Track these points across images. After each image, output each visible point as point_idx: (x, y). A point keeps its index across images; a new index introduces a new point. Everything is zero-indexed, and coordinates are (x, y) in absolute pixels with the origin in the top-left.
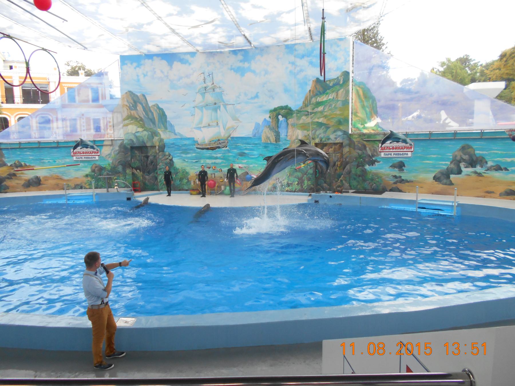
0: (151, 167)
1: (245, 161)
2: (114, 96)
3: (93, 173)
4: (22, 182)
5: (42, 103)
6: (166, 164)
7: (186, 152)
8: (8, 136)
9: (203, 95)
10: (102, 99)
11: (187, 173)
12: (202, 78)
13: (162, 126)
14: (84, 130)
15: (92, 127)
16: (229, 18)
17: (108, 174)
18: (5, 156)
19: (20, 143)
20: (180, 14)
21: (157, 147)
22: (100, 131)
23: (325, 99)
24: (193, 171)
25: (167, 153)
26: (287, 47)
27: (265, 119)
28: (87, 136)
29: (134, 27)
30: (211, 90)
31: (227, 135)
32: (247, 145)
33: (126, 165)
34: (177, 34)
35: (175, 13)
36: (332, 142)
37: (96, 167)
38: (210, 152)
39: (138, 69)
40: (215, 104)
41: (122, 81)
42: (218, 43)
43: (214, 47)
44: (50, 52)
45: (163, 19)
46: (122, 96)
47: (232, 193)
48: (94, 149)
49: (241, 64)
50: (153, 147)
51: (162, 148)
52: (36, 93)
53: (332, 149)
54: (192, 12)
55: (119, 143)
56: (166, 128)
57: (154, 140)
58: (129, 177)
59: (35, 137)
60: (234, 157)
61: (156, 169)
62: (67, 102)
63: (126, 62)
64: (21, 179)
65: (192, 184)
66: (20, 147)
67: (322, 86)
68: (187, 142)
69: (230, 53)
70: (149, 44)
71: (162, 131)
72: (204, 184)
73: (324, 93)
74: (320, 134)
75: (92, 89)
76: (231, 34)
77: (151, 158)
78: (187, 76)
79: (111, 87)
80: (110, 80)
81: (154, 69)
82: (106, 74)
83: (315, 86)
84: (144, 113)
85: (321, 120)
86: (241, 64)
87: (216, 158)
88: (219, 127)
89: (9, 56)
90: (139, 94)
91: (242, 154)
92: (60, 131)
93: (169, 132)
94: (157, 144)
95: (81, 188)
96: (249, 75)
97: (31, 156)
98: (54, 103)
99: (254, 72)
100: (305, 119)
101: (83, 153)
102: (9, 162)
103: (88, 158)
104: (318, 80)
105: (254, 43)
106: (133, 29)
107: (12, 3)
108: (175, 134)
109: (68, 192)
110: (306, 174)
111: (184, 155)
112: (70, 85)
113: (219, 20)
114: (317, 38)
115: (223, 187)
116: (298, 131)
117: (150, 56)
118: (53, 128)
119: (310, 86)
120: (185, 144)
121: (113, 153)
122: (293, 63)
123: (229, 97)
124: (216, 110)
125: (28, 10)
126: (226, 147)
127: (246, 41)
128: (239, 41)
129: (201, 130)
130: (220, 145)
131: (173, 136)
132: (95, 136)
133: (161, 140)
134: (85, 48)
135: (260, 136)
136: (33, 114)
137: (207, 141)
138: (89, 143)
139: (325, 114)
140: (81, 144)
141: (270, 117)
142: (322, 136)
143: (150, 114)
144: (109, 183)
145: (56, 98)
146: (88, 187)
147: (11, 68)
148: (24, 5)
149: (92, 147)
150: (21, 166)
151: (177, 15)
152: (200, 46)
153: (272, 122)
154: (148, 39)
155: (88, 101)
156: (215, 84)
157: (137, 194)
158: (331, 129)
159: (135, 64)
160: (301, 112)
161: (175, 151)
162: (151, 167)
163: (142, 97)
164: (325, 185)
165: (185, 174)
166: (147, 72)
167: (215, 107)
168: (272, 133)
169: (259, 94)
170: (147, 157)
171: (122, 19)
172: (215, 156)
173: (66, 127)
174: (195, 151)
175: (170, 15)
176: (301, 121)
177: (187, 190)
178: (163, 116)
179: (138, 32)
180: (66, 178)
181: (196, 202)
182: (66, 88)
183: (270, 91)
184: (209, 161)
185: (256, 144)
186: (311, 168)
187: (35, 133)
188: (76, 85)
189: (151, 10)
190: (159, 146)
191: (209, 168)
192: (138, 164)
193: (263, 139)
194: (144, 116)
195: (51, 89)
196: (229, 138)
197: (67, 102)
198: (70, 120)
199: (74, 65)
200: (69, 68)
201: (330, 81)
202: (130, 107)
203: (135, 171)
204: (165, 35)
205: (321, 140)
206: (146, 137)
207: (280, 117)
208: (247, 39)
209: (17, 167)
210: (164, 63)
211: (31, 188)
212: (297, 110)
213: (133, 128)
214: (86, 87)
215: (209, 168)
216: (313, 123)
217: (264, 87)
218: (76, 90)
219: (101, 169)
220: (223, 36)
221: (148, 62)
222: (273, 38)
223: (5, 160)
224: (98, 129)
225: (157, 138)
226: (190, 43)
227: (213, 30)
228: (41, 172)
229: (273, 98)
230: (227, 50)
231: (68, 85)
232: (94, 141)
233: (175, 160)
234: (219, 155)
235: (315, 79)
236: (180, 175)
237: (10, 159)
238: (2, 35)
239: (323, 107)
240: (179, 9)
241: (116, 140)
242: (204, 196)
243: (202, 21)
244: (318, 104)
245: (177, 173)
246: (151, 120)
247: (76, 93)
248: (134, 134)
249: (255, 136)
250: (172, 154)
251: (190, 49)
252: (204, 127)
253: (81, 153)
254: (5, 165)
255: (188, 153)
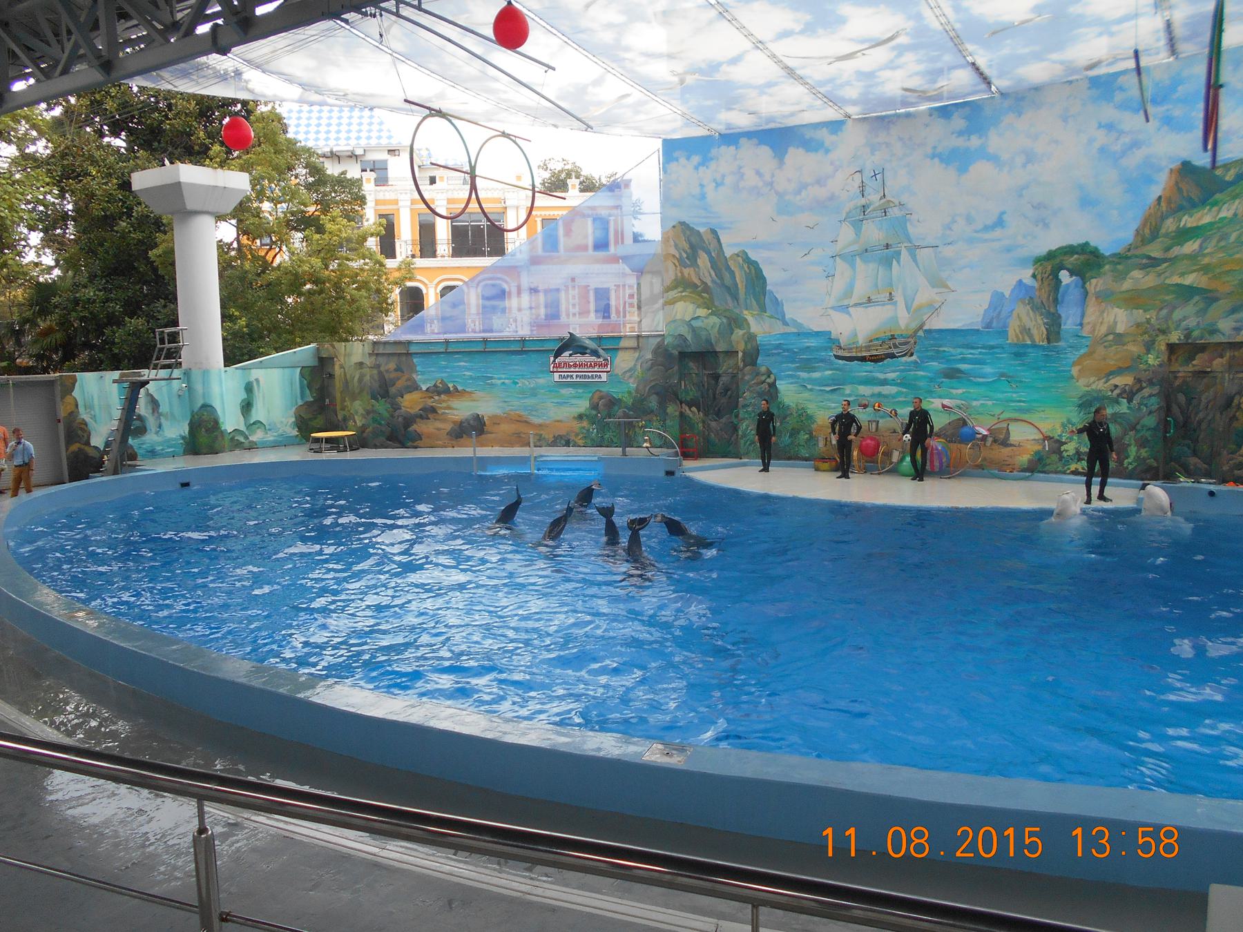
0: (724, 400)
1: (960, 391)
2: (641, 235)
3: (594, 412)
4: (448, 427)
5: (490, 255)
6: (760, 395)
7: (808, 365)
8: (420, 328)
9: (857, 225)
10: (616, 242)
11: (810, 417)
12: (858, 182)
13: (754, 303)
14: (574, 315)
15: (592, 307)
16: (935, 25)
17: (626, 416)
18: (418, 368)
19: (447, 342)
20: (809, 30)
21: (740, 354)
22: (609, 317)
23: (1207, 219)
24: (824, 412)
25: (763, 369)
26: (1095, 82)
27: (1020, 281)
28: (584, 325)
29: (700, 71)
30: (879, 213)
31: (914, 325)
32: (964, 351)
33: (667, 394)
34: (801, 79)
35: (798, 28)
36: (1224, 340)
37: (601, 398)
38: (869, 366)
39: (701, 169)
40: (887, 246)
41: (666, 199)
42: (900, 92)
43: (890, 102)
44: (518, 140)
45: (771, 46)
46: (663, 234)
47: (919, 474)
48: (599, 357)
49: (960, 142)
50: (732, 353)
51: (752, 356)
52: (478, 230)
53: (1224, 360)
54: (842, 21)
55: (655, 341)
56: (763, 309)
57: (734, 337)
58: (673, 423)
59: (473, 328)
60: (931, 380)
61: (737, 407)
62: (540, 251)
63: (676, 154)
64: (445, 420)
65: (821, 444)
66: (447, 350)
67: (1198, 184)
68: (812, 343)
69: (931, 115)
70: (730, 109)
71: (753, 316)
72: (847, 448)
73: (1203, 202)
74: (1185, 318)
75: (594, 220)
76: (939, 65)
77: (724, 380)
78: (820, 182)
79: (636, 214)
80: (634, 198)
81: (740, 168)
82: (627, 184)
83: (1177, 183)
84: (713, 273)
85: (1189, 280)
86: (960, 142)
87: (884, 383)
88: (895, 303)
89: (430, 156)
90: (702, 230)
91: (953, 374)
92: (525, 317)
93: (771, 317)
94: (741, 347)
95: (567, 444)
96: (980, 169)
97: (469, 370)
98: (513, 255)
99: (994, 159)
100: (1138, 279)
101: (575, 365)
102: (425, 381)
103: (585, 377)
104: (1186, 169)
105: (999, 83)
106: (697, 76)
107: (449, 40)
108: (785, 323)
109: (538, 451)
110: (1133, 428)
111: (803, 375)
112: (547, 213)
113: (907, 34)
114: (1196, 49)
115: (896, 456)
116: (1116, 310)
117: (731, 138)
118: (510, 308)
119: (1162, 186)
120: (808, 347)
121: (639, 367)
122: (1110, 127)
123: (925, 227)
124: (887, 262)
125: (478, 53)
126: (912, 355)
127: (976, 79)
128: (962, 78)
129: (848, 313)
130: (895, 351)
131: (779, 328)
132: (600, 326)
133: (751, 337)
134: (589, 127)
135: (1005, 326)
136: (472, 280)
137: (861, 341)
138: (588, 343)
139: (1206, 260)
140: (571, 344)
141: (1034, 276)
142: (1192, 322)
143: (727, 275)
144: (627, 435)
145: (517, 244)
146: (581, 442)
147: (433, 181)
148: (469, 42)
149: (595, 353)
150: (447, 391)
151: (802, 32)
152: (854, 103)
153: (1040, 289)
154: (729, 95)
155: (585, 248)
156: (888, 198)
157: (688, 464)
158: (1224, 304)
159: (696, 159)
160: (1127, 258)
161: (782, 363)
162: (724, 400)
163: (711, 236)
164: (1193, 461)
165: (805, 418)
166: (723, 176)
167: (887, 254)
168: (1039, 318)
169: (1005, 217)
170: (716, 377)
171: (670, 56)
172: (881, 376)
173: (537, 307)
174: (831, 363)
175: (785, 34)
176: (1127, 285)
177: (806, 459)
178: (756, 278)
179: (707, 82)
180: (536, 420)
181: (821, 487)
182: (539, 220)
183: (1038, 207)
184: (865, 390)
185: (992, 347)
186: (1150, 413)
187: (474, 322)
188: (560, 213)
189: (741, 28)
190: (744, 352)
191: (865, 406)
192: (693, 393)
193: (1011, 333)
194: (713, 281)
195: (510, 223)
196: (921, 333)
197: (540, 251)
198: (547, 291)
199: (558, 166)
200: (547, 175)
201: (1227, 167)
202: (680, 260)
203: (686, 408)
204: (770, 85)
205: (1188, 336)
206: (716, 330)
207: (1064, 276)
208: (981, 74)
209: (439, 394)
210: (765, 151)
211: (464, 440)
212: (1114, 255)
213: (685, 310)
214: (584, 216)
215: (865, 406)
216: (1167, 289)
217: (1021, 196)
218: (560, 223)
219: (612, 402)
220: (917, 74)
221: (727, 152)
222: (1054, 62)
223: (418, 378)
224: (605, 311)
225: (741, 332)
226: (831, 100)
227: (892, 61)
228: (486, 406)
229: (1046, 225)
230: (924, 107)
231: (543, 213)
232: (600, 338)
233: (782, 386)
234: (891, 376)
235: (1175, 165)
236: (792, 422)
237: (426, 377)
238: (428, 112)
239: (1199, 241)
240: (808, 17)
241: (648, 337)
242: (845, 475)
243: (863, 42)
244: (1184, 235)
245: (785, 418)
246: (728, 289)
247: (561, 232)
248: (689, 324)
249: (988, 326)
250: (774, 371)
251: (830, 114)
252: (856, 305)
253: (570, 366)
254: (414, 387)
255: (814, 370)
